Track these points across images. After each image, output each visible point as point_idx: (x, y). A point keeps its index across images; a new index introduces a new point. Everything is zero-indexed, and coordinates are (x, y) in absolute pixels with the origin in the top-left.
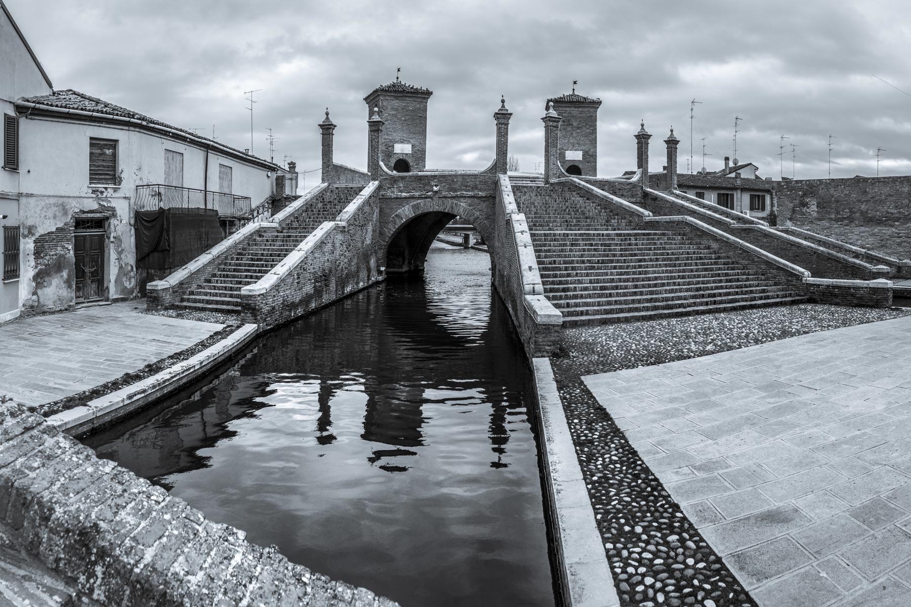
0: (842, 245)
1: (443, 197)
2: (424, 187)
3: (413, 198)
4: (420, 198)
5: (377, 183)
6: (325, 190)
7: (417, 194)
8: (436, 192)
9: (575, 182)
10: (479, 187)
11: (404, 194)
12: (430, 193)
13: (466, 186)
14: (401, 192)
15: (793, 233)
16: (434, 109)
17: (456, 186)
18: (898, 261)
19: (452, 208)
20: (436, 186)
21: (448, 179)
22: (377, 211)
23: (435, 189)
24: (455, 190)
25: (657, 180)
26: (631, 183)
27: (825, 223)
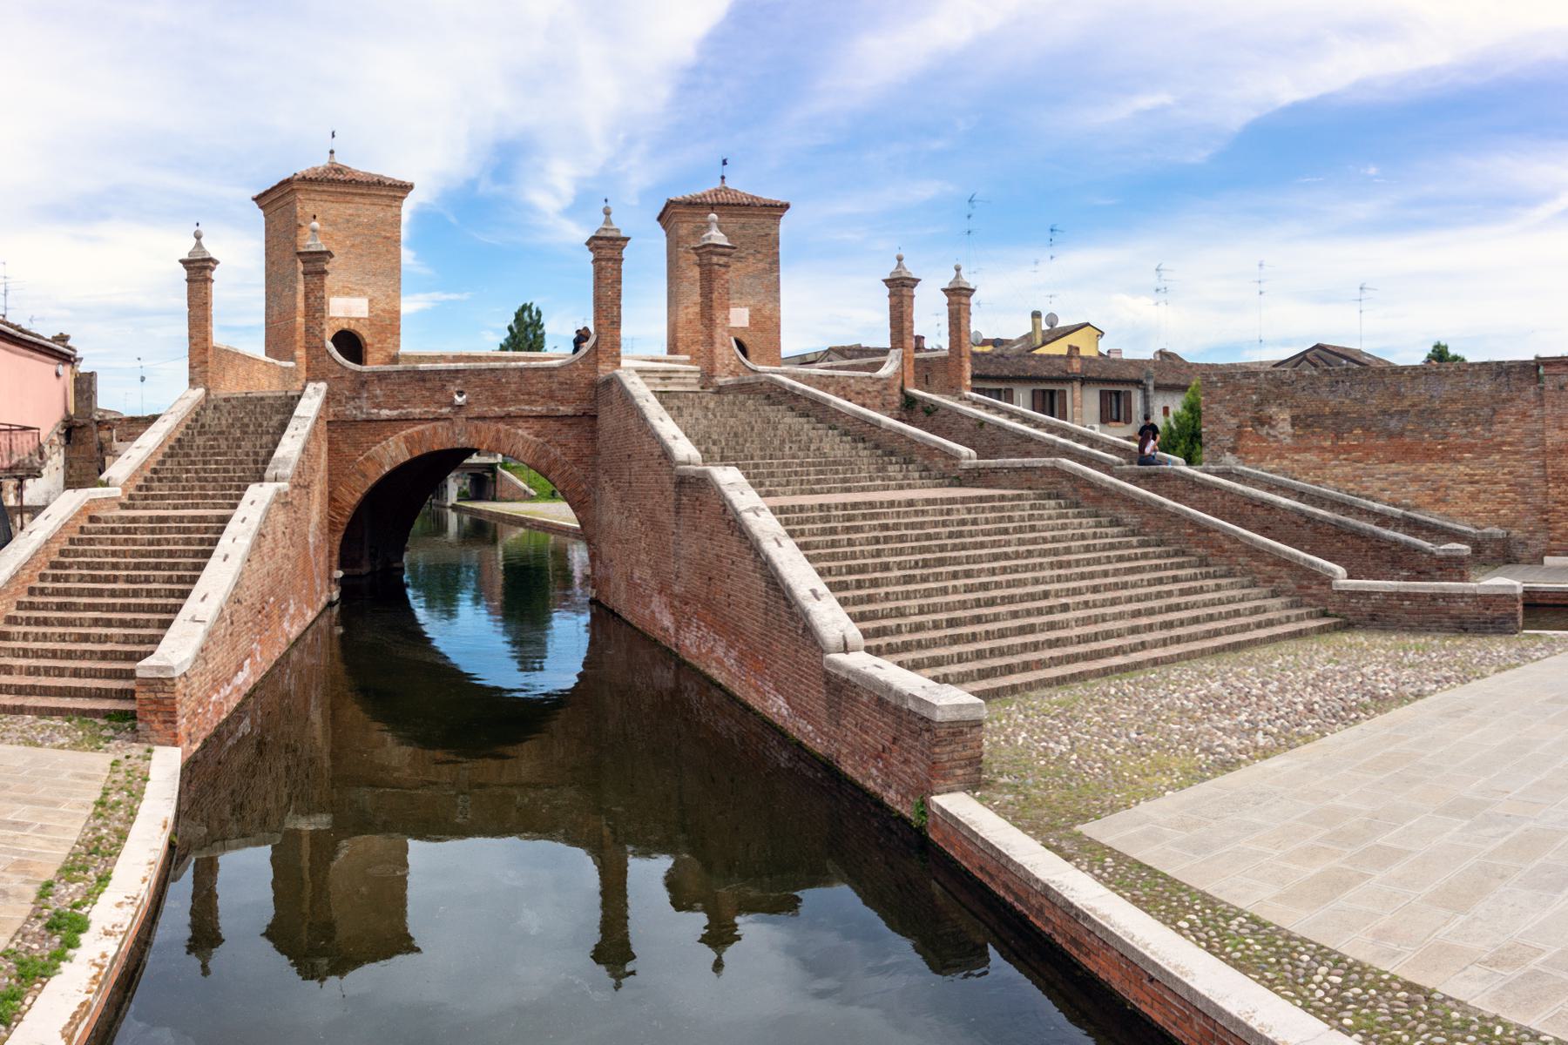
0: (1351, 501)
1: (478, 418)
2: (432, 396)
4: (421, 420)
7: (417, 411)
8: (460, 406)
9: (783, 383)
10: (559, 394)
11: (385, 413)
13: (529, 394)
14: (378, 406)
15: (1240, 477)
18: (1473, 531)
19: (498, 440)
20: (460, 393)
23: (459, 400)
24: (502, 401)
25: (929, 369)
26: (880, 379)
27: (1311, 457)
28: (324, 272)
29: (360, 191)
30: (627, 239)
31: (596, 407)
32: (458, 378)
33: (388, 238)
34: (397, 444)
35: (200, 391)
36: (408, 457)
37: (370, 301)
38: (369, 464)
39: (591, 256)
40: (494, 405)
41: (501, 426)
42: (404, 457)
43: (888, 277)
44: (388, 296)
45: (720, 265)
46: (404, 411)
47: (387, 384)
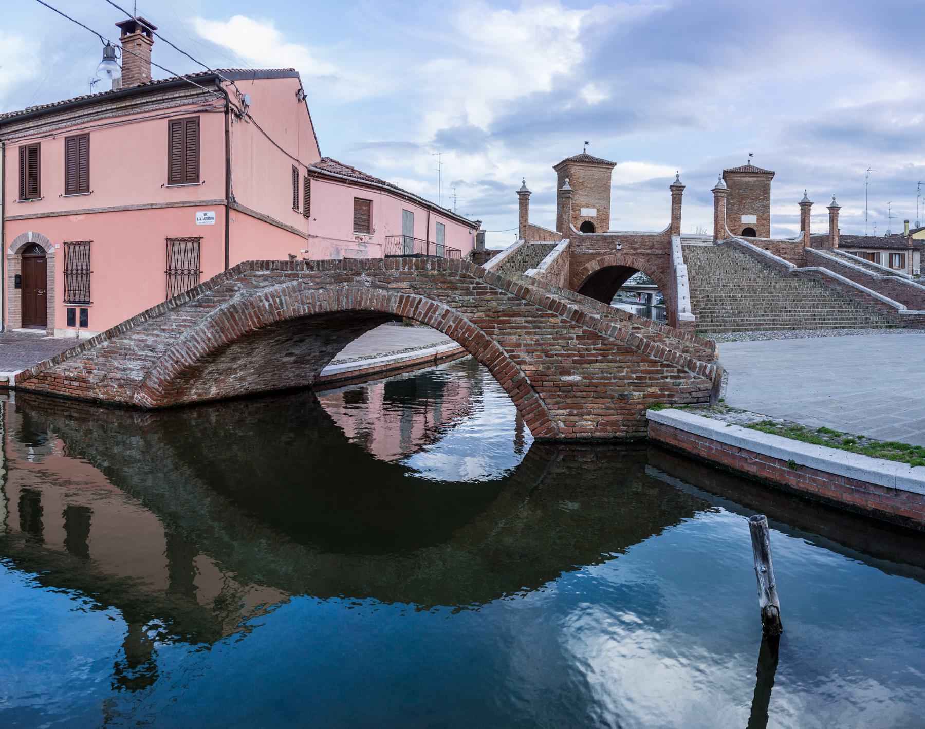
3: (599, 254)
5: (568, 241)
6: (523, 246)
7: (602, 251)
10: (656, 246)
11: (591, 251)
12: (613, 251)
14: (589, 249)
16: (617, 176)
17: (636, 245)
19: (633, 263)
20: (619, 245)
21: (628, 239)
22: (568, 263)
23: (618, 247)
24: (635, 249)
30: (684, 187)
35: (523, 241)
37: (597, 210)
39: (671, 193)
42: (598, 268)
44: (605, 208)
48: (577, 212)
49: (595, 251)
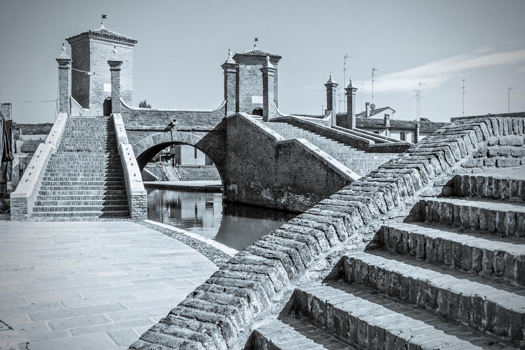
2: (164, 121)
7: (158, 127)
11: (144, 127)
19: (189, 139)
24: (191, 124)
28: (120, 70)
29: (116, 41)
31: (226, 128)
32: (173, 115)
33: (127, 61)
34: (150, 140)
36: (154, 145)
38: (138, 147)
40: (188, 125)
41: (190, 133)
43: (326, 83)
45: (271, 76)
46: (153, 127)
47: (145, 116)
48: (100, 87)
49: (149, 127)
